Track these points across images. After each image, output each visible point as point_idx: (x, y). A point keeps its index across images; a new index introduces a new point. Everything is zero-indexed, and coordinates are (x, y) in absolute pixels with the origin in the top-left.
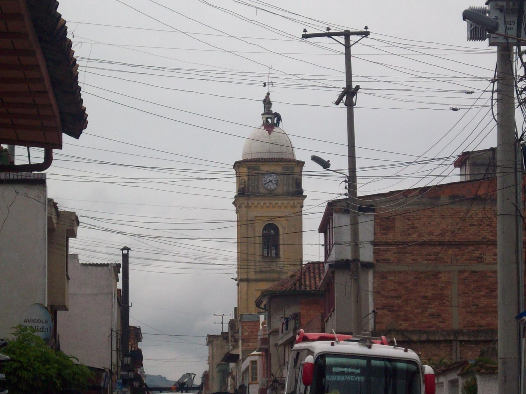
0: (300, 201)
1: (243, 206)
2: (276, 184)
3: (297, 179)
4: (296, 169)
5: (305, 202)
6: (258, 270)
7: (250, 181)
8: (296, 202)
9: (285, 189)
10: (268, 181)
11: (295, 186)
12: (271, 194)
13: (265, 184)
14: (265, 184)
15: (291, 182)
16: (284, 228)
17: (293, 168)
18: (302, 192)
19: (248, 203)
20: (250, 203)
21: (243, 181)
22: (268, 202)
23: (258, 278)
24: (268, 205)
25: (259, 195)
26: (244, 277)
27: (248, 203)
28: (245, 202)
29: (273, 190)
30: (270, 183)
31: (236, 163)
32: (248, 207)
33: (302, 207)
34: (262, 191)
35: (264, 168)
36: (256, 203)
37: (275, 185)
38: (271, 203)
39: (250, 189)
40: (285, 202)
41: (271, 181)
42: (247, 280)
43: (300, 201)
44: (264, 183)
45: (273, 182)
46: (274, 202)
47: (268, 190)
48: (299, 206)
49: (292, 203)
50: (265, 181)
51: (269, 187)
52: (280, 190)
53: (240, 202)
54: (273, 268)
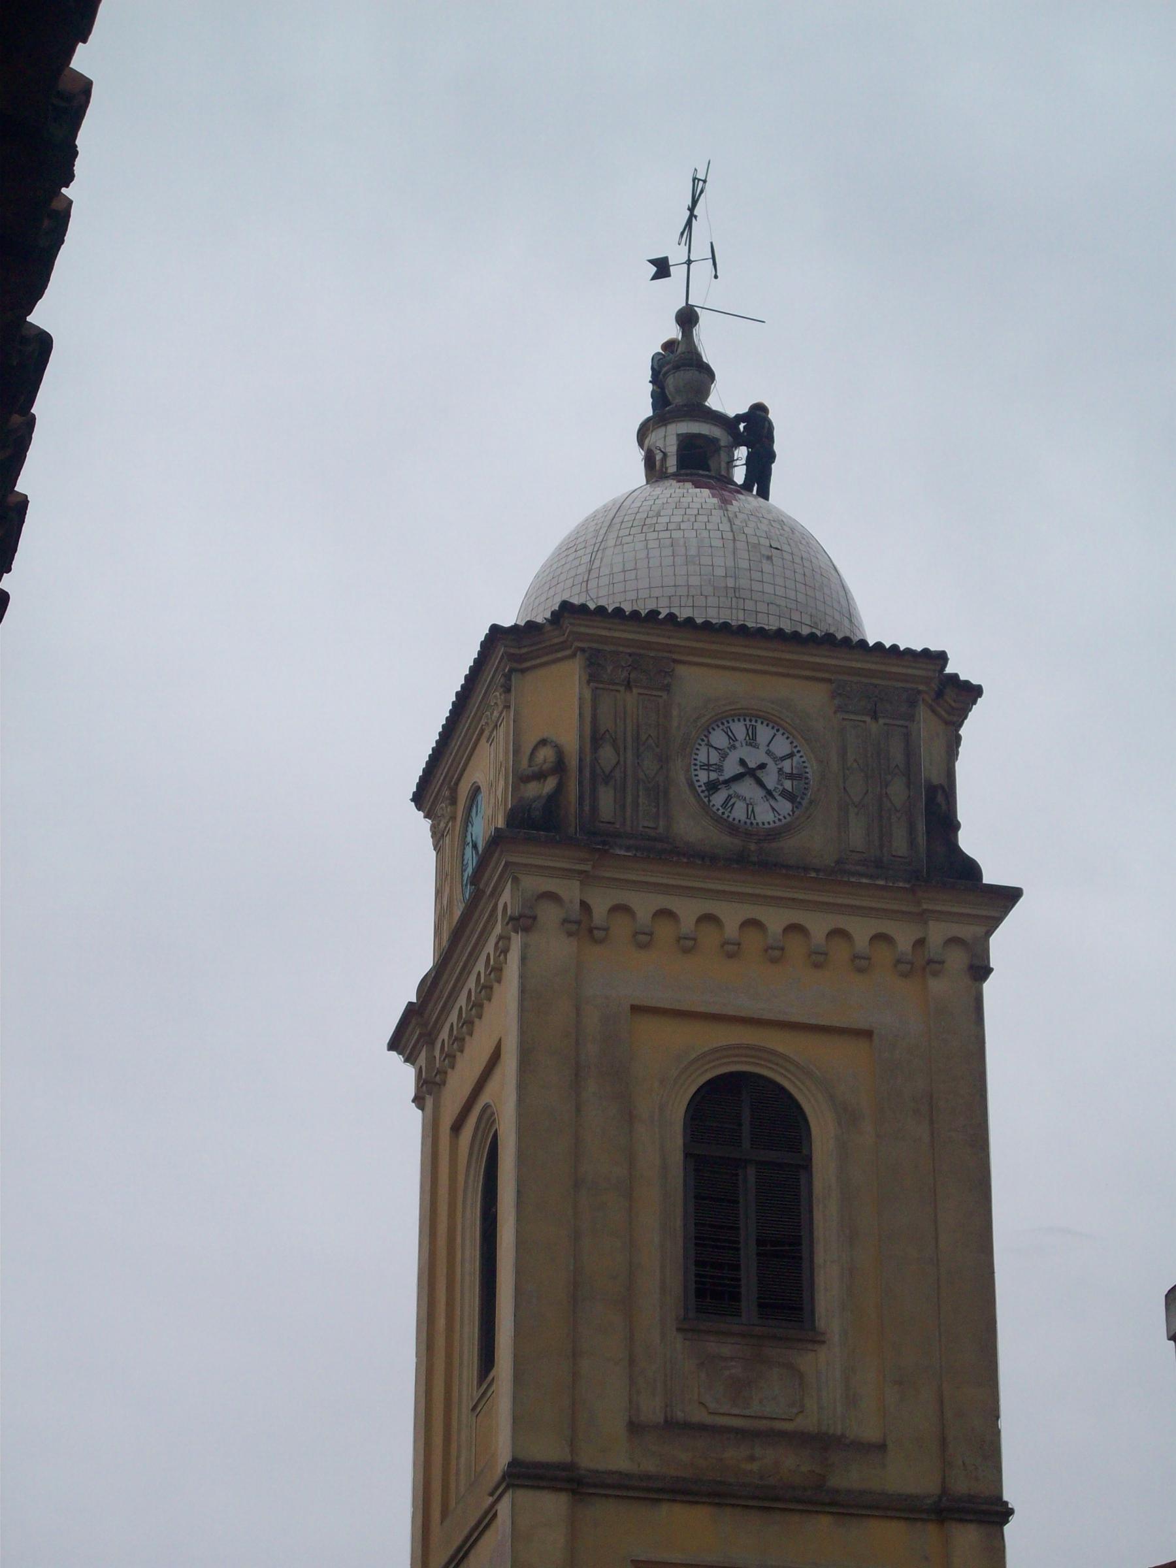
0: (966, 931)
1: (549, 915)
2: (789, 796)
3: (932, 790)
4: (926, 724)
5: (1004, 944)
6: (652, 1409)
7: (607, 754)
8: (937, 932)
9: (857, 835)
10: (731, 768)
11: (921, 826)
12: (753, 857)
13: (713, 787)
14: (713, 787)
15: (897, 791)
16: (848, 1116)
17: (913, 704)
18: (971, 870)
19: (585, 907)
20: (601, 904)
21: (546, 755)
22: (732, 915)
23: (650, 1466)
24: (731, 929)
25: (662, 851)
26: (547, 1450)
27: (583, 904)
28: (570, 891)
29: (773, 834)
30: (747, 789)
31: (496, 633)
32: (582, 927)
33: (982, 971)
34: (689, 827)
35: (700, 684)
36: (644, 905)
37: (785, 806)
38: (752, 923)
39: (606, 801)
40: (862, 930)
41: (751, 773)
42: (570, 1481)
43: (966, 931)
44: (703, 777)
45: (770, 779)
46: (775, 920)
47: (733, 828)
48: (957, 960)
49: (904, 937)
50: (707, 767)
51: (739, 813)
52: (816, 841)
53: (534, 884)
54: (771, 1400)
